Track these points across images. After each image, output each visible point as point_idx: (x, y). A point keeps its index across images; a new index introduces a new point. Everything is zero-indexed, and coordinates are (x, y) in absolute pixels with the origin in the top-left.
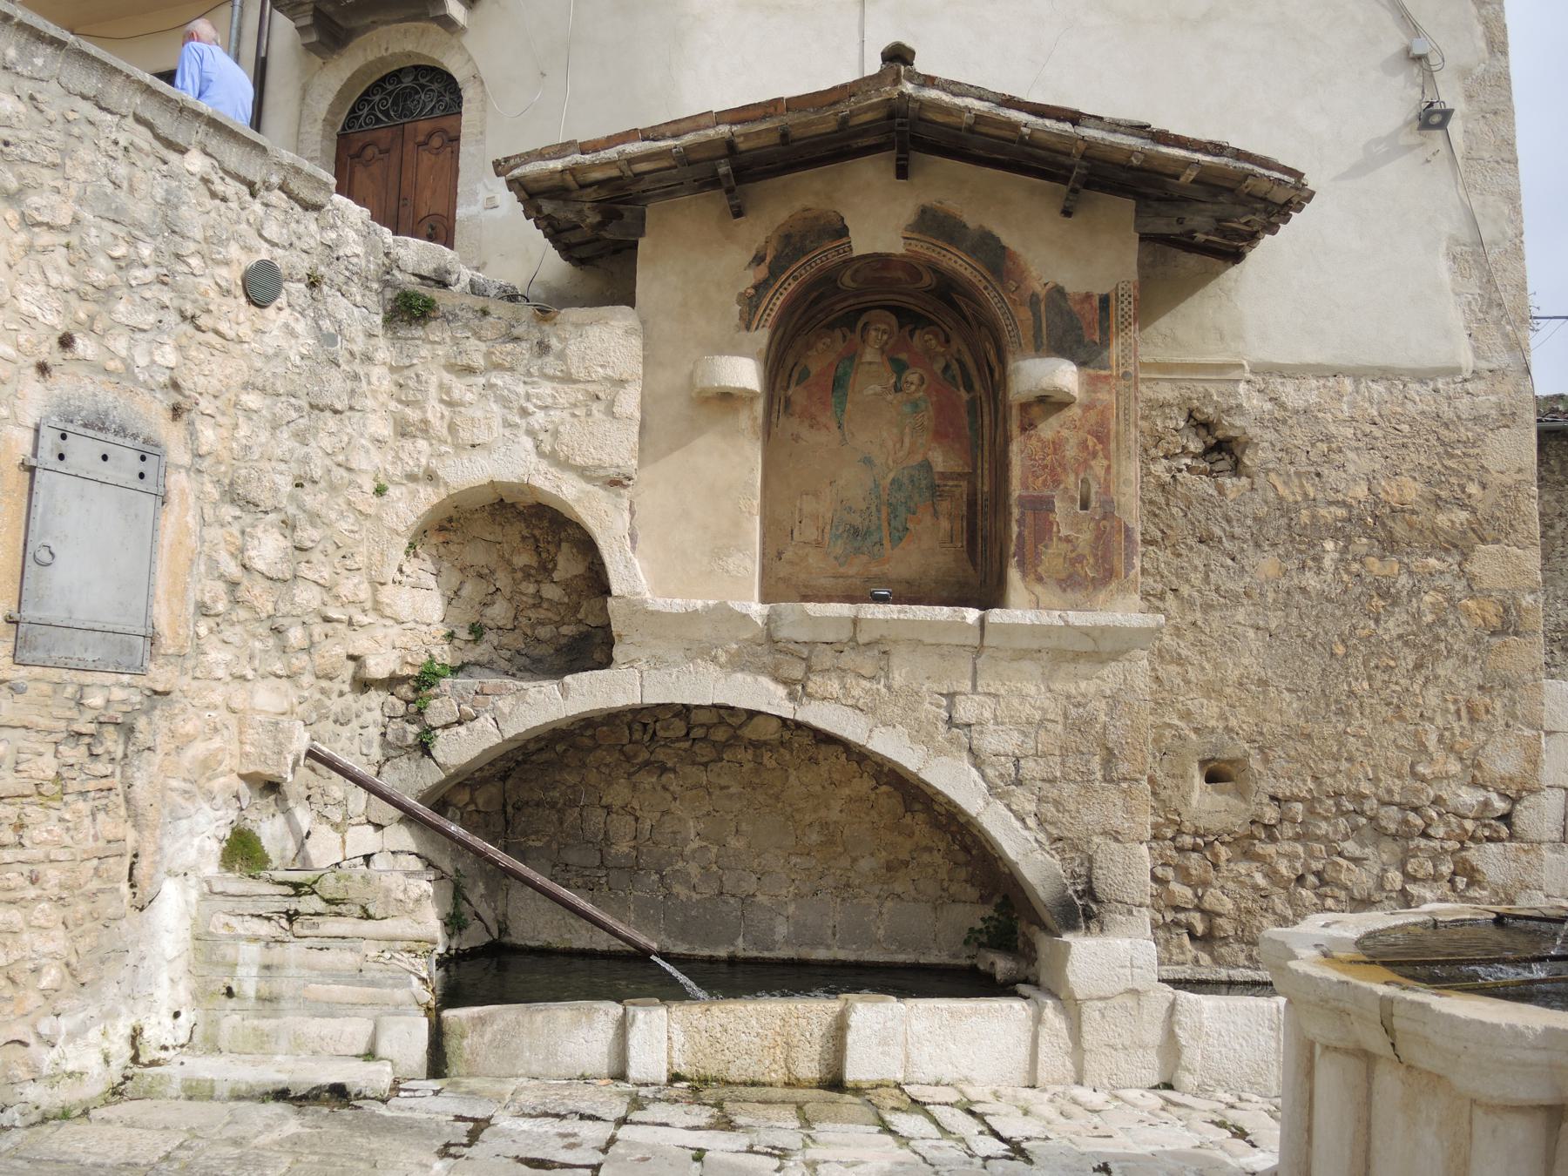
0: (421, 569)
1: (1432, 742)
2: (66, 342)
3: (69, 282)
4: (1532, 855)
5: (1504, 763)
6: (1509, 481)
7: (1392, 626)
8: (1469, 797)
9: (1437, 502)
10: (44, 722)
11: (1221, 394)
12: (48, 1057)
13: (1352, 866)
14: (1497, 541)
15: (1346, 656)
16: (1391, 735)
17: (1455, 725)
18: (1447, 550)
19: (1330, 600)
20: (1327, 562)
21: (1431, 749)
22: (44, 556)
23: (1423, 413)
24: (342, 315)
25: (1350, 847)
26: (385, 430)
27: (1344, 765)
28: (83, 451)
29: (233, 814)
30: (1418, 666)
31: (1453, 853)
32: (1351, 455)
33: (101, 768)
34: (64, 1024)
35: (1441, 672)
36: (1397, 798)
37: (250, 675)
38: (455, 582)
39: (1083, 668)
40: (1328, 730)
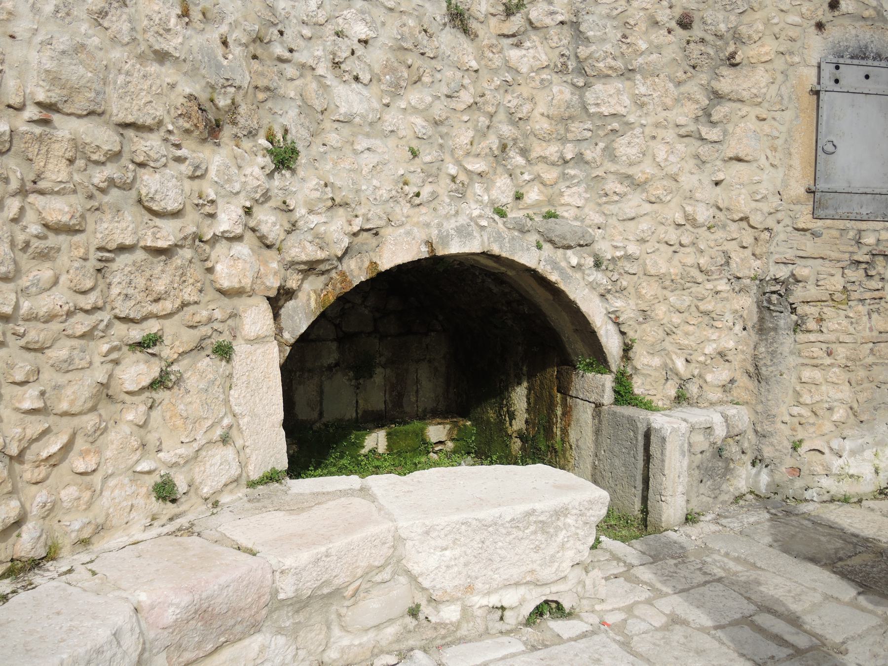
10: (835, 255)
12: (836, 464)
22: (829, 148)
28: (851, 75)
33: (874, 284)
34: (848, 445)
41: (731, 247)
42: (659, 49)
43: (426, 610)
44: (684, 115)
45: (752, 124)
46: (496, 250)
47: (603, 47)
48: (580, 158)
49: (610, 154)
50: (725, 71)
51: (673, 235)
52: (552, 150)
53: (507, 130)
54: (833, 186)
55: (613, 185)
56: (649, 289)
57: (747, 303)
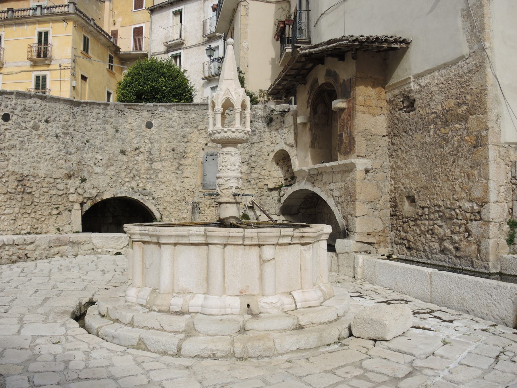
0: (278, 168)
1: (457, 188)
2: (206, 144)
3: (206, 136)
4: (486, 226)
5: (477, 193)
6: (478, 91)
7: (447, 150)
8: (467, 205)
9: (459, 105)
11: (407, 88)
13: (439, 228)
14: (475, 114)
15: (436, 161)
16: (447, 185)
17: (464, 181)
18: (461, 121)
19: (432, 144)
20: (432, 132)
21: (457, 189)
23: (455, 75)
24: (257, 126)
25: (439, 222)
26: (269, 144)
27: (436, 196)
29: (243, 211)
30: (454, 162)
31: (465, 224)
32: (437, 96)
35: (460, 163)
36: (449, 206)
37: (244, 189)
38: (286, 169)
39: (347, 174)
40: (432, 185)
41: (185, 195)
42: (167, 156)
43: (95, 249)
44: (173, 168)
45: (189, 170)
46: (128, 196)
47: (156, 156)
48: (150, 178)
49: (157, 176)
50: (182, 159)
51: (171, 193)
52: (145, 176)
53: (135, 172)
54: (206, 182)
55: (158, 183)
56: (166, 204)
57: (190, 207)
